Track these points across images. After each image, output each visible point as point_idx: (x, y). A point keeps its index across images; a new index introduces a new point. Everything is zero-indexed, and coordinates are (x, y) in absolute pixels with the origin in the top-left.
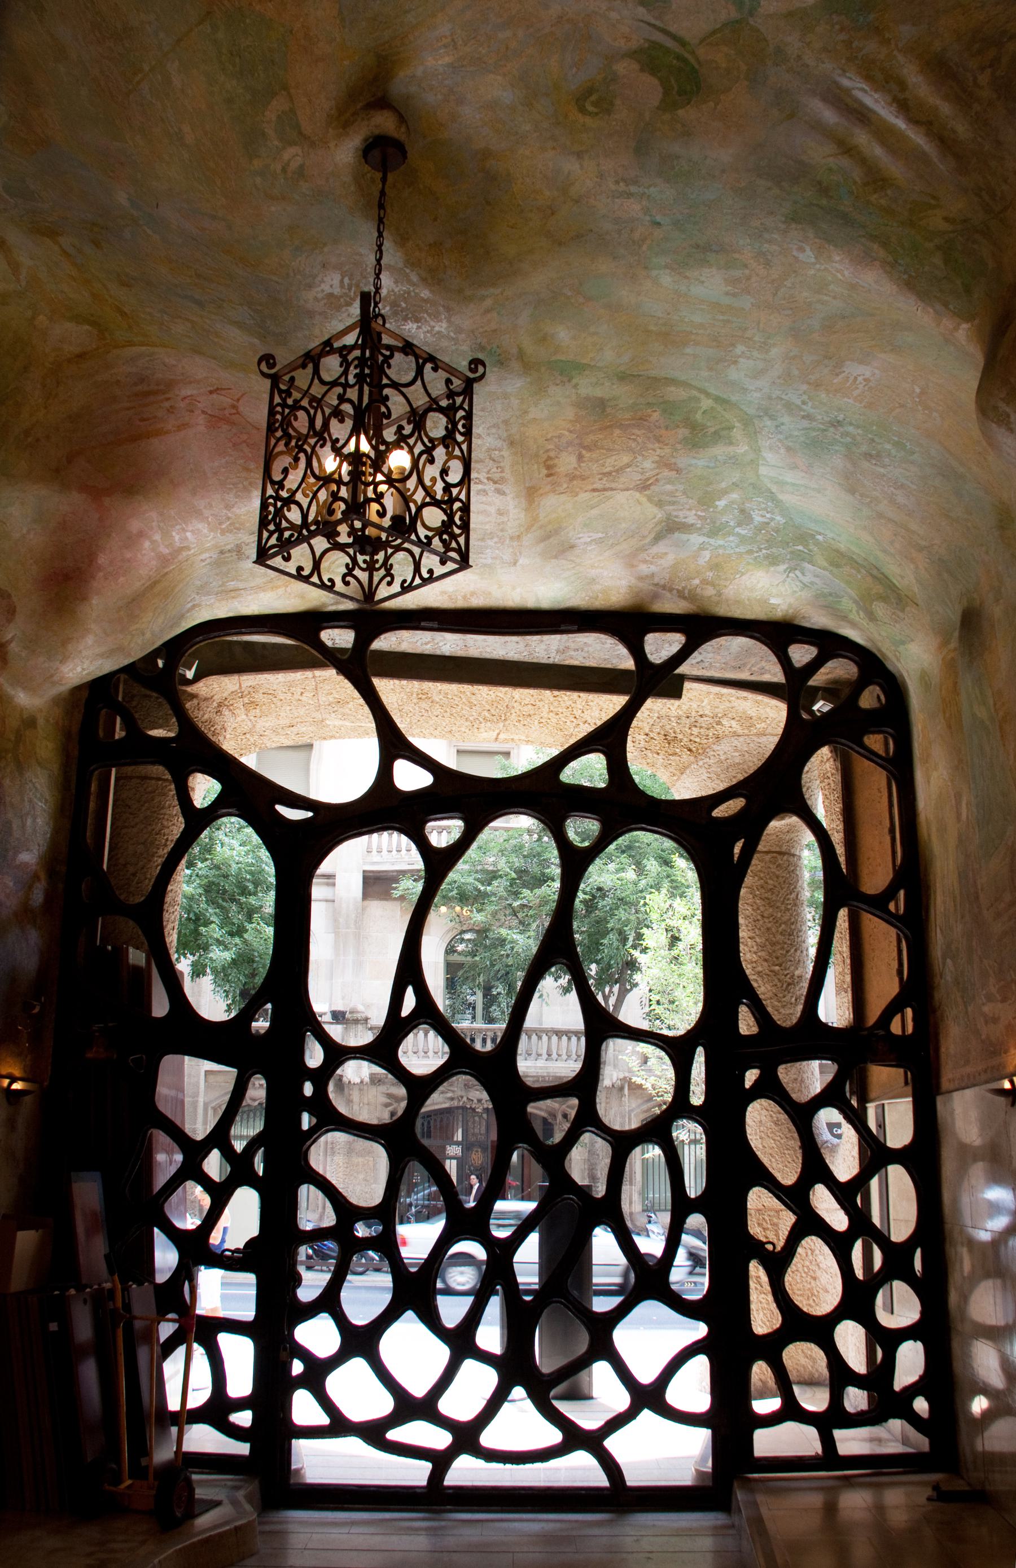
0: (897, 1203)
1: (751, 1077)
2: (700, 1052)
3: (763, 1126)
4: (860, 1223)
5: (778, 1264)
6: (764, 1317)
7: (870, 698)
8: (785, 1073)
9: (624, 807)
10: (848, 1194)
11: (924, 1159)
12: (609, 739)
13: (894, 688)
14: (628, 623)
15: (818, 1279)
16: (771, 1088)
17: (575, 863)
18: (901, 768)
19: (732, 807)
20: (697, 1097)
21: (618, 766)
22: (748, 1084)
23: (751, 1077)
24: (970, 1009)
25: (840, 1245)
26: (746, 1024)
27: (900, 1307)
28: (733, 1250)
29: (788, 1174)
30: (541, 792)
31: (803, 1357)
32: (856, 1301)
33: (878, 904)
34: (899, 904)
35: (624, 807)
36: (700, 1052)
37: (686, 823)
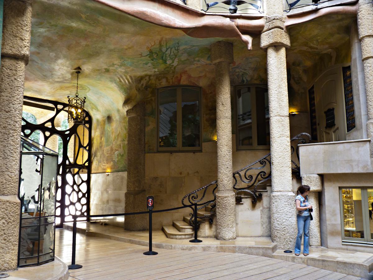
0: (84, 188)
1: (68, 170)
2: (61, 166)
3: (69, 177)
4: (80, 190)
5: (69, 195)
6: (67, 203)
7: (87, 119)
8: (72, 170)
9: (53, 131)
10: (78, 186)
11: (88, 182)
12: (52, 120)
13: (90, 118)
14: (56, 103)
15: (74, 198)
16: (70, 172)
17: (46, 138)
18: (90, 129)
19: (67, 133)
20: (61, 173)
21: (53, 125)
22: (67, 171)
23: (68, 170)
24: (100, 164)
25: (78, 193)
26: (67, 162)
27: (84, 201)
28: (64, 194)
29: (71, 183)
30: (42, 128)
31: (71, 207)
32: (79, 200)
33: (85, 148)
34: (87, 148)
35: (53, 131)
36: (61, 166)
37: (61, 134)
